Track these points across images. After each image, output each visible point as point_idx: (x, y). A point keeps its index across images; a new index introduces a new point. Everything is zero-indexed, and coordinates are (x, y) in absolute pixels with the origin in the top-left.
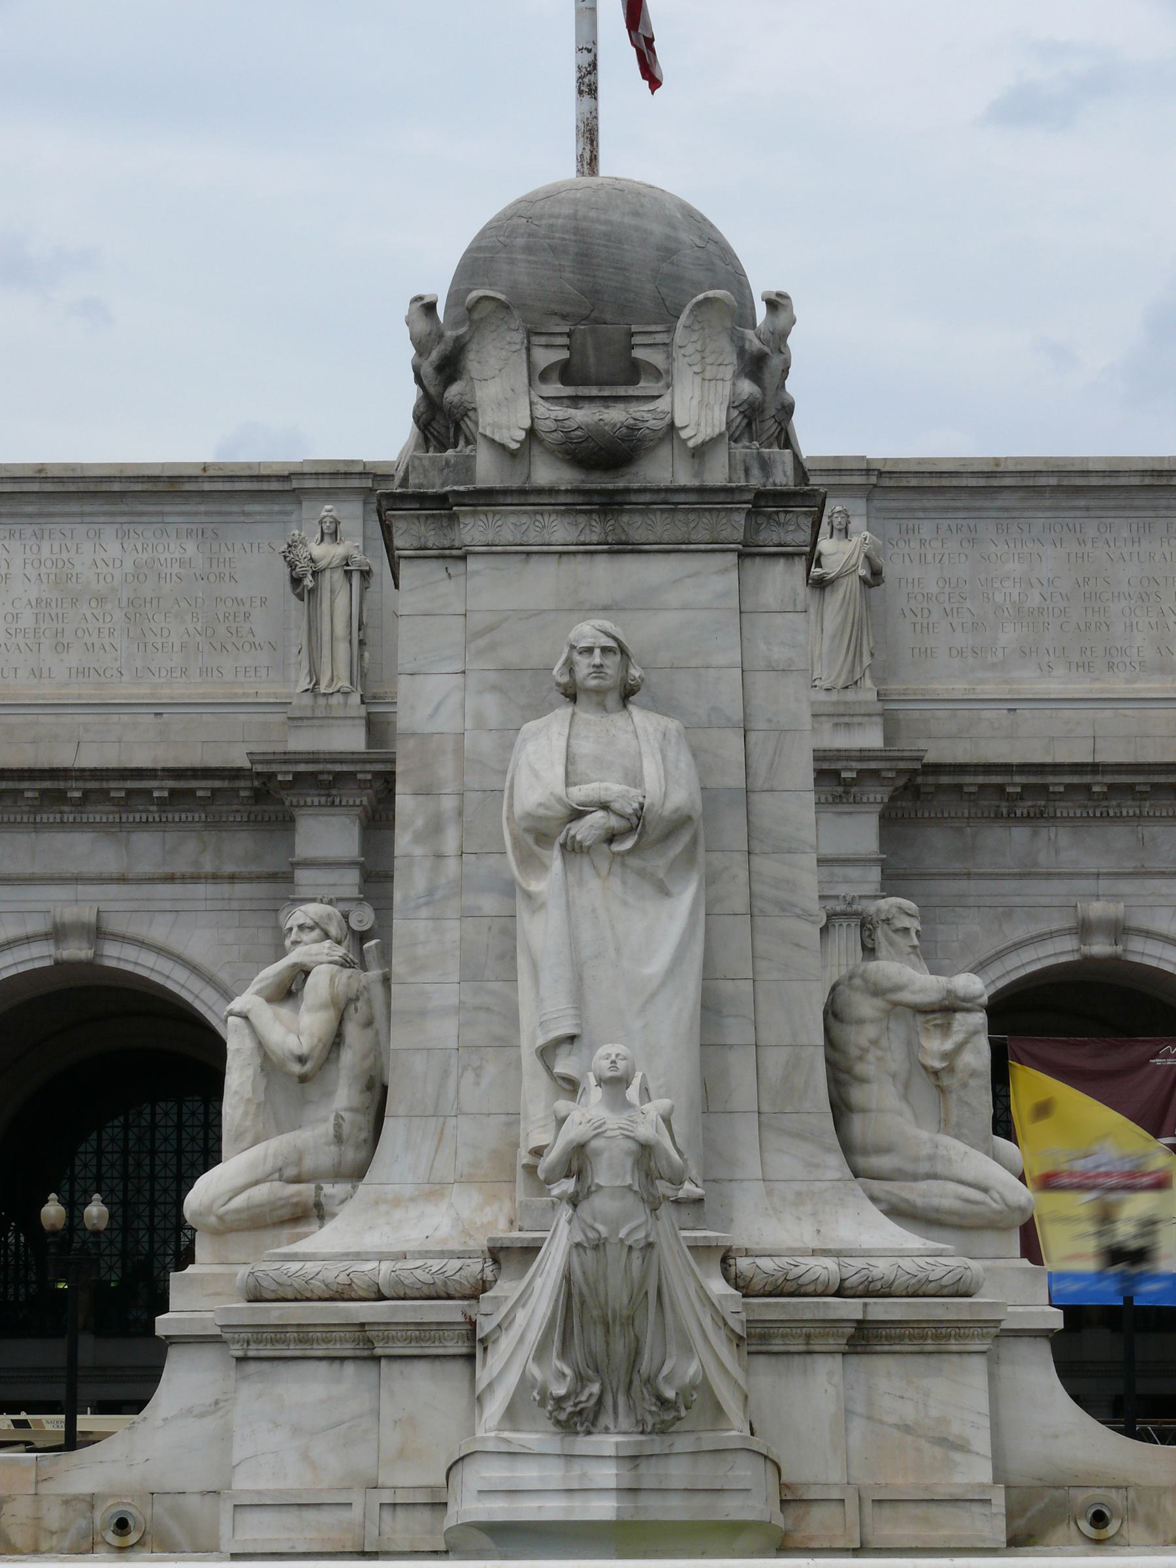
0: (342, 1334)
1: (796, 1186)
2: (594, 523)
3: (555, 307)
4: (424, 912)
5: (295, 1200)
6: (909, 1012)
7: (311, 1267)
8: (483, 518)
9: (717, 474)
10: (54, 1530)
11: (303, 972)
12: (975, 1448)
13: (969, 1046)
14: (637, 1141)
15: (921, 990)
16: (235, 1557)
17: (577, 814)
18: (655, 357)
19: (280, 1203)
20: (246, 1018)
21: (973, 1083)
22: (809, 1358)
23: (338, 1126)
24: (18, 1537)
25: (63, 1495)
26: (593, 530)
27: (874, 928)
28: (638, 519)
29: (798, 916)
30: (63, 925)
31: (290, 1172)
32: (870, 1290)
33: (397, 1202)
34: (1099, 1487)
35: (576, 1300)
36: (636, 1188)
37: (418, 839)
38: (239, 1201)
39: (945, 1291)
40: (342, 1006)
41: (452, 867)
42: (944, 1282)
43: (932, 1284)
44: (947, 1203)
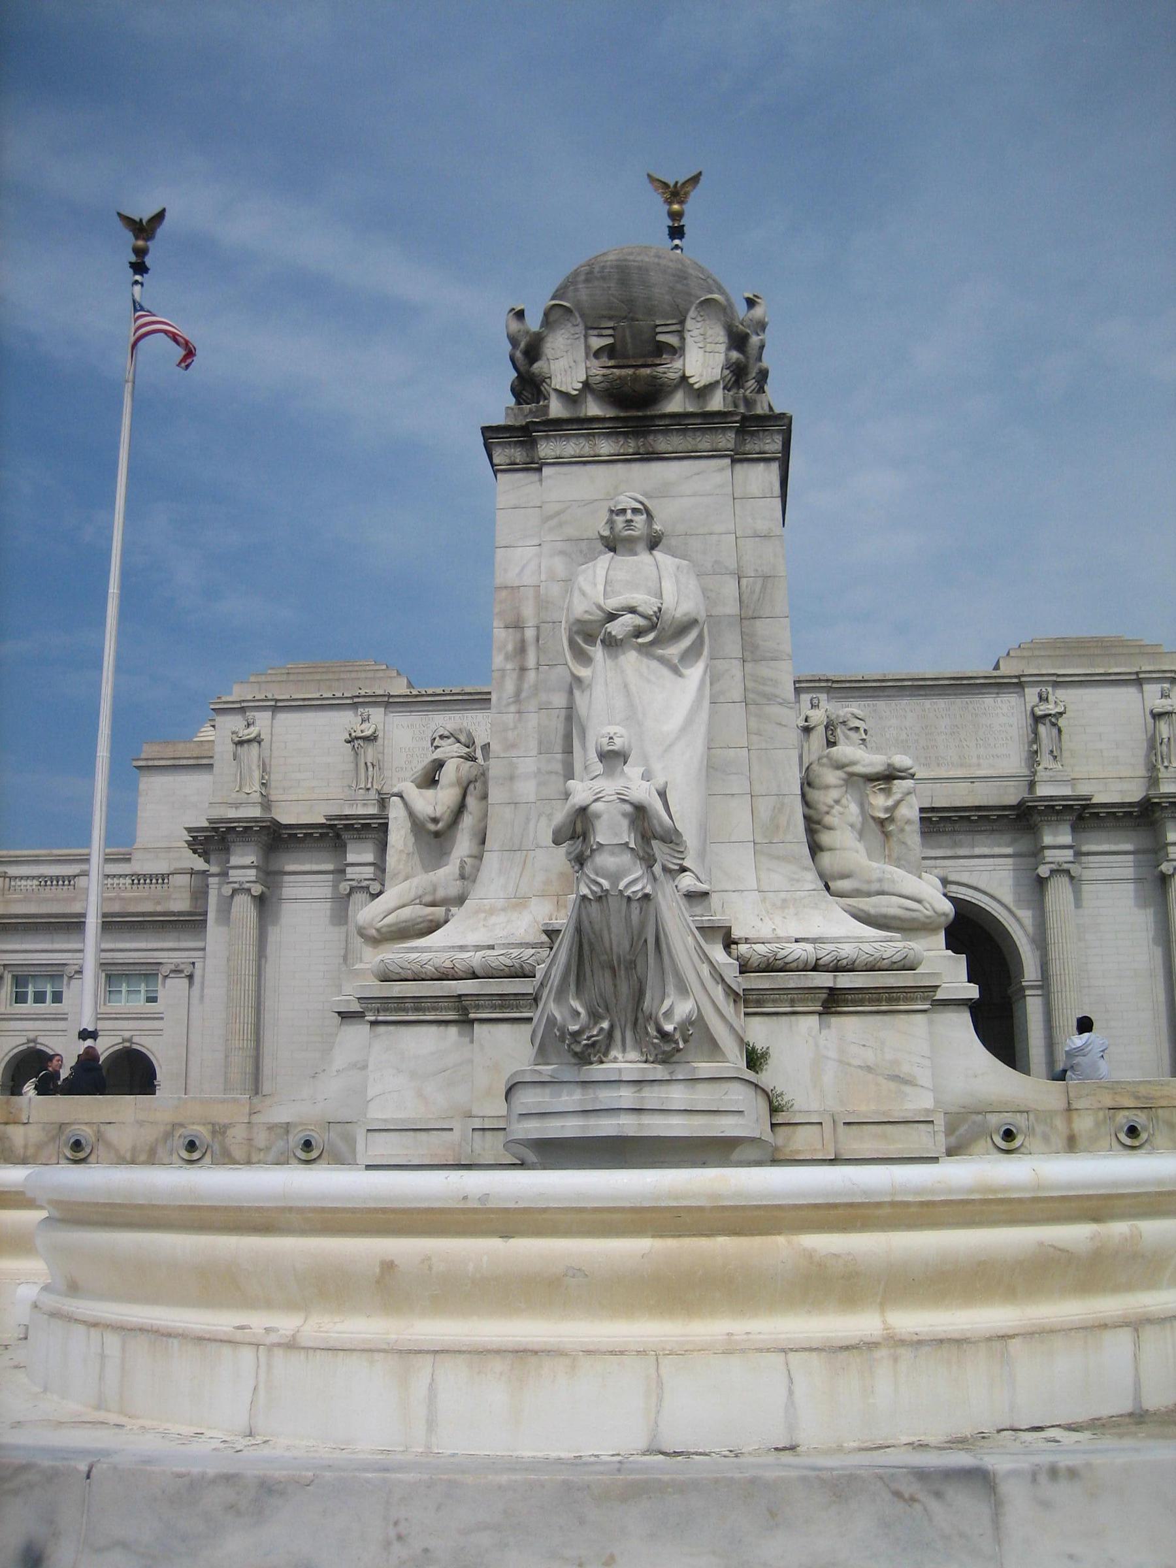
0: (446, 1004)
1: (783, 895)
2: (630, 441)
3: (605, 313)
4: (513, 708)
5: (430, 918)
6: (861, 780)
7: (425, 956)
8: (553, 440)
9: (717, 402)
10: (262, 1148)
11: (439, 765)
12: (920, 1083)
14: (631, 804)
16: (369, 1167)
17: (612, 617)
18: (673, 340)
19: (420, 920)
20: (401, 797)
21: (907, 828)
22: (793, 1018)
23: (462, 868)
24: (238, 1153)
25: (268, 1123)
26: (631, 445)
27: (836, 729)
28: (661, 438)
29: (780, 704)
30: (460, 875)
31: (428, 899)
32: (838, 968)
33: (492, 911)
34: (1007, 1112)
35: (586, 947)
36: (632, 845)
37: (507, 658)
38: (390, 919)
39: (895, 966)
40: (465, 784)
41: (531, 676)
42: (894, 959)
43: (885, 961)
44: (893, 911)
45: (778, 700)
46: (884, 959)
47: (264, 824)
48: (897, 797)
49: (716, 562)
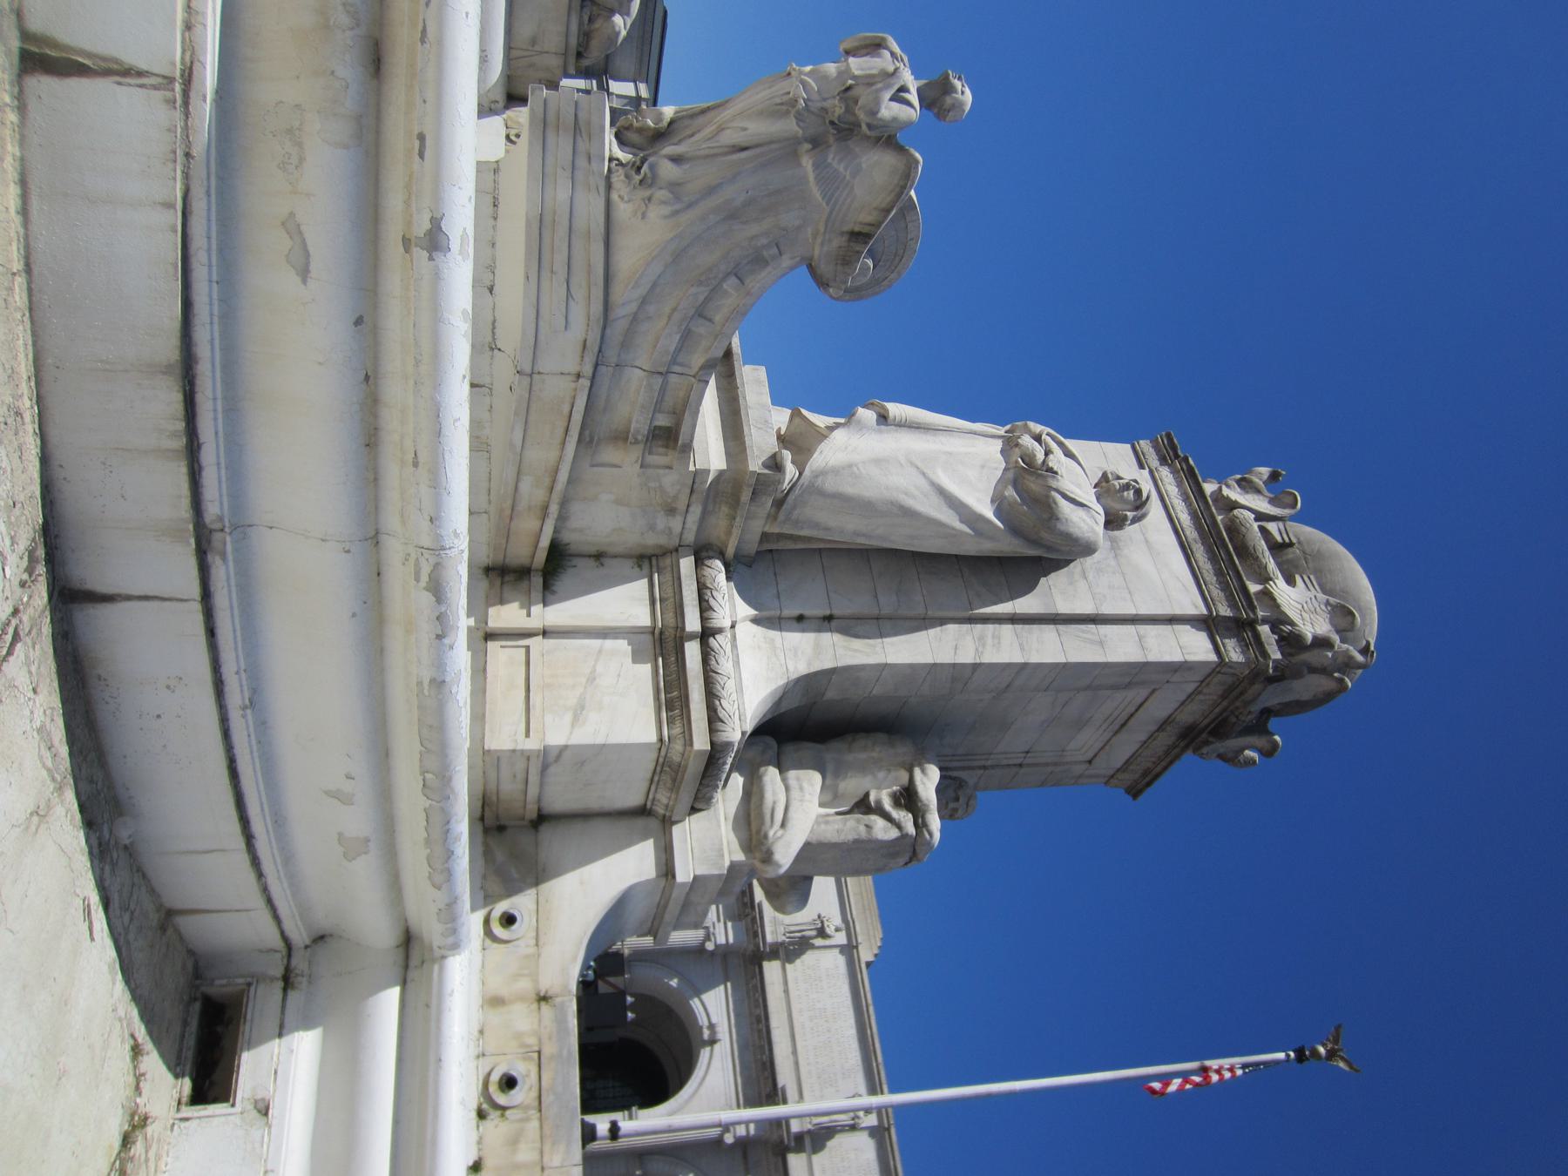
3: (1302, 539)
13: (890, 825)
15: (924, 784)
34: (537, 921)
42: (719, 708)
45: (980, 649)
46: (720, 701)
49: (1105, 596)
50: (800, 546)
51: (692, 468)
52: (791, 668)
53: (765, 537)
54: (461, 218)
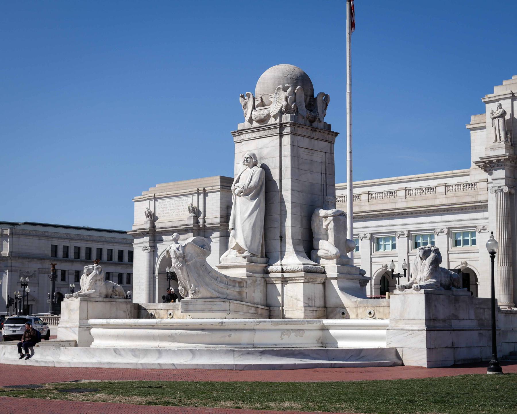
47: (505, 158)
48: (328, 222)
50: (264, 247)
51: (246, 278)
52: (292, 250)
53: (262, 257)
54: (219, 320)
